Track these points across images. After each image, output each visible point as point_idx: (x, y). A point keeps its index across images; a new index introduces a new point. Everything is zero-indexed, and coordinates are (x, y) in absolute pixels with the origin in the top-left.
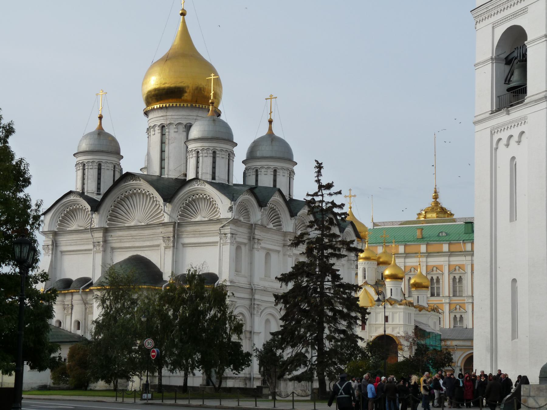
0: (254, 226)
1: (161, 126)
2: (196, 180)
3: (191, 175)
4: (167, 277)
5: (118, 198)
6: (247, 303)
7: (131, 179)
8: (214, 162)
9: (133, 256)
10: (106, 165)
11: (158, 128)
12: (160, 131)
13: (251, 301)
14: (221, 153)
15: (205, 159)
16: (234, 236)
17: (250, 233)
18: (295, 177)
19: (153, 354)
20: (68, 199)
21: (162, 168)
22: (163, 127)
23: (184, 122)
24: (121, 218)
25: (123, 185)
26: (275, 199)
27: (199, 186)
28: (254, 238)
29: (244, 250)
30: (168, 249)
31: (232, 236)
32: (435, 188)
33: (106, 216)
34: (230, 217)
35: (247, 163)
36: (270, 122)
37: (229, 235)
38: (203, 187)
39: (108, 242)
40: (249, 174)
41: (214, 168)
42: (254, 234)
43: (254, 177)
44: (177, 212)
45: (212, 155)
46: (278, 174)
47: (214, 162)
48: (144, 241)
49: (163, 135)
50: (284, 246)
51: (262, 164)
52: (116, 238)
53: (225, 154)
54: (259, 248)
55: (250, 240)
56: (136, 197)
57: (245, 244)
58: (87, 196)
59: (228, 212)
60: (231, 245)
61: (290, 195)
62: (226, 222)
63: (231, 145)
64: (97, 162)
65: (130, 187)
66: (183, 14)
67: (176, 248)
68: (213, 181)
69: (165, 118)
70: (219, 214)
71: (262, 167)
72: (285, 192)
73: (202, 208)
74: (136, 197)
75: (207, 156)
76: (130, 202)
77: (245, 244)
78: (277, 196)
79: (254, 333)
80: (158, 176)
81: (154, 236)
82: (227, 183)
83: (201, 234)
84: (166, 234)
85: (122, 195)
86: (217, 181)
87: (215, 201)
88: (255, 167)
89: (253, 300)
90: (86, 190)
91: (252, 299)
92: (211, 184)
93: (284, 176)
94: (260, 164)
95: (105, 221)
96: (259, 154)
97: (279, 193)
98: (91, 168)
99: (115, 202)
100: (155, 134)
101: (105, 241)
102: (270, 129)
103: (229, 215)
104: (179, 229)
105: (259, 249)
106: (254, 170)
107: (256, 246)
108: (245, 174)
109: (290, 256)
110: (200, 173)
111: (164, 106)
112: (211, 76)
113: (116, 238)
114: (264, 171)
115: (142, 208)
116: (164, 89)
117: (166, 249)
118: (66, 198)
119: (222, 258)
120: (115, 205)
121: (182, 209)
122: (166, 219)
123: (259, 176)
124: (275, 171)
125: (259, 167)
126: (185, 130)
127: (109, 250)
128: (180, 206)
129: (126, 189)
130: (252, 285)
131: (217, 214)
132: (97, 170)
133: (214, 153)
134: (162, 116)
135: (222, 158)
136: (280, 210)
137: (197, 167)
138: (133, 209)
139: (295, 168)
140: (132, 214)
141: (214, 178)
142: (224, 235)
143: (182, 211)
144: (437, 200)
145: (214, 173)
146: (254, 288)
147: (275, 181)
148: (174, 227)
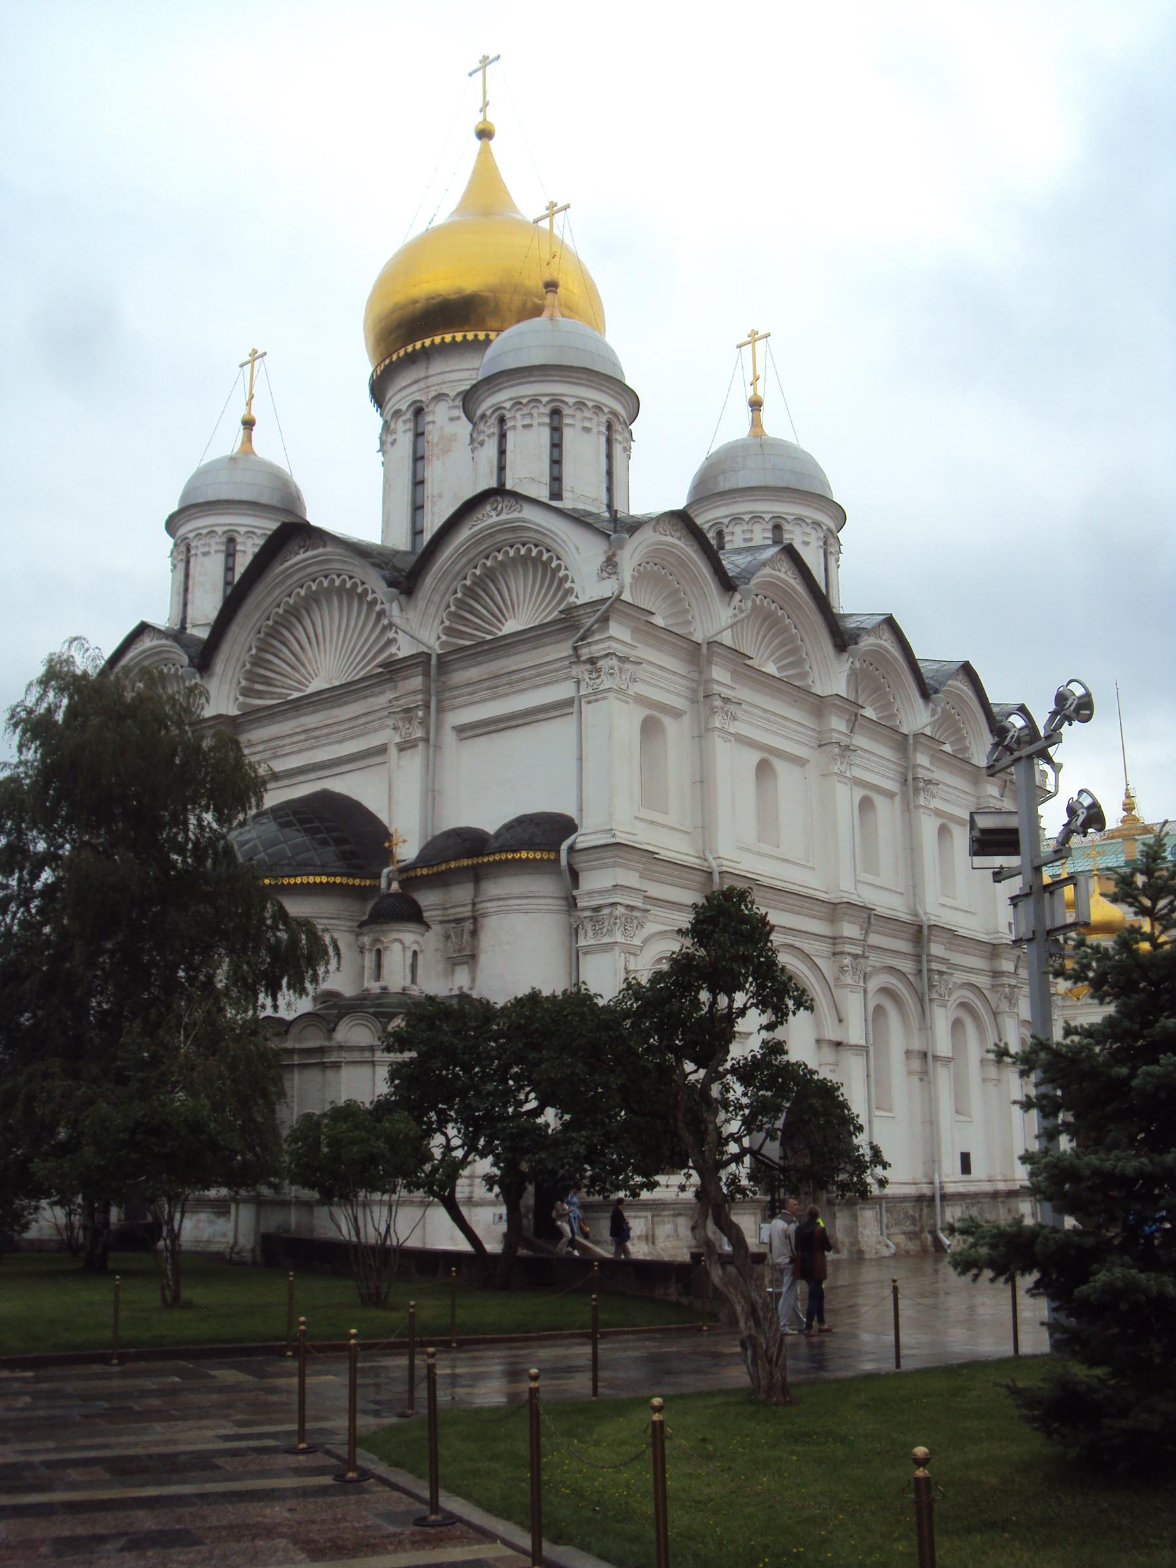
1: (412, 409)
2: (492, 499)
4: (408, 850)
5: (268, 619)
7: (301, 547)
8: (556, 445)
10: (250, 542)
14: (579, 414)
15: (529, 435)
16: (627, 666)
20: (137, 651)
25: (277, 571)
26: (779, 578)
27: (504, 517)
30: (409, 752)
32: (1127, 790)
33: (235, 681)
38: (515, 515)
41: (556, 462)
44: (437, 621)
45: (547, 420)
47: (556, 445)
48: (342, 741)
49: (419, 435)
50: (820, 746)
51: (735, 512)
52: (260, 748)
53: (595, 417)
55: (694, 701)
56: (320, 609)
57: (676, 714)
62: (593, 619)
65: (295, 578)
66: (485, 134)
68: (554, 504)
69: (422, 385)
71: (736, 519)
74: (320, 609)
75: (530, 426)
76: (305, 630)
77: (676, 714)
78: (786, 573)
81: (370, 718)
83: (515, 682)
84: (401, 702)
85: (278, 606)
86: (567, 503)
87: (558, 558)
95: (232, 697)
98: (206, 554)
99: (259, 632)
100: (395, 440)
102: (756, 423)
104: (443, 679)
113: (260, 748)
114: (743, 531)
117: (403, 753)
118: (132, 649)
120: (258, 644)
121: (453, 608)
125: (726, 521)
129: (289, 582)
130: (710, 858)
132: (221, 557)
133: (556, 413)
134: (416, 382)
135: (587, 430)
136: (800, 627)
138: (312, 650)
140: (310, 664)
141: (556, 495)
142: (588, 667)
143: (454, 616)
144: (1133, 813)
145: (556, 480)
146: (716, 869)
148: (426, 674)
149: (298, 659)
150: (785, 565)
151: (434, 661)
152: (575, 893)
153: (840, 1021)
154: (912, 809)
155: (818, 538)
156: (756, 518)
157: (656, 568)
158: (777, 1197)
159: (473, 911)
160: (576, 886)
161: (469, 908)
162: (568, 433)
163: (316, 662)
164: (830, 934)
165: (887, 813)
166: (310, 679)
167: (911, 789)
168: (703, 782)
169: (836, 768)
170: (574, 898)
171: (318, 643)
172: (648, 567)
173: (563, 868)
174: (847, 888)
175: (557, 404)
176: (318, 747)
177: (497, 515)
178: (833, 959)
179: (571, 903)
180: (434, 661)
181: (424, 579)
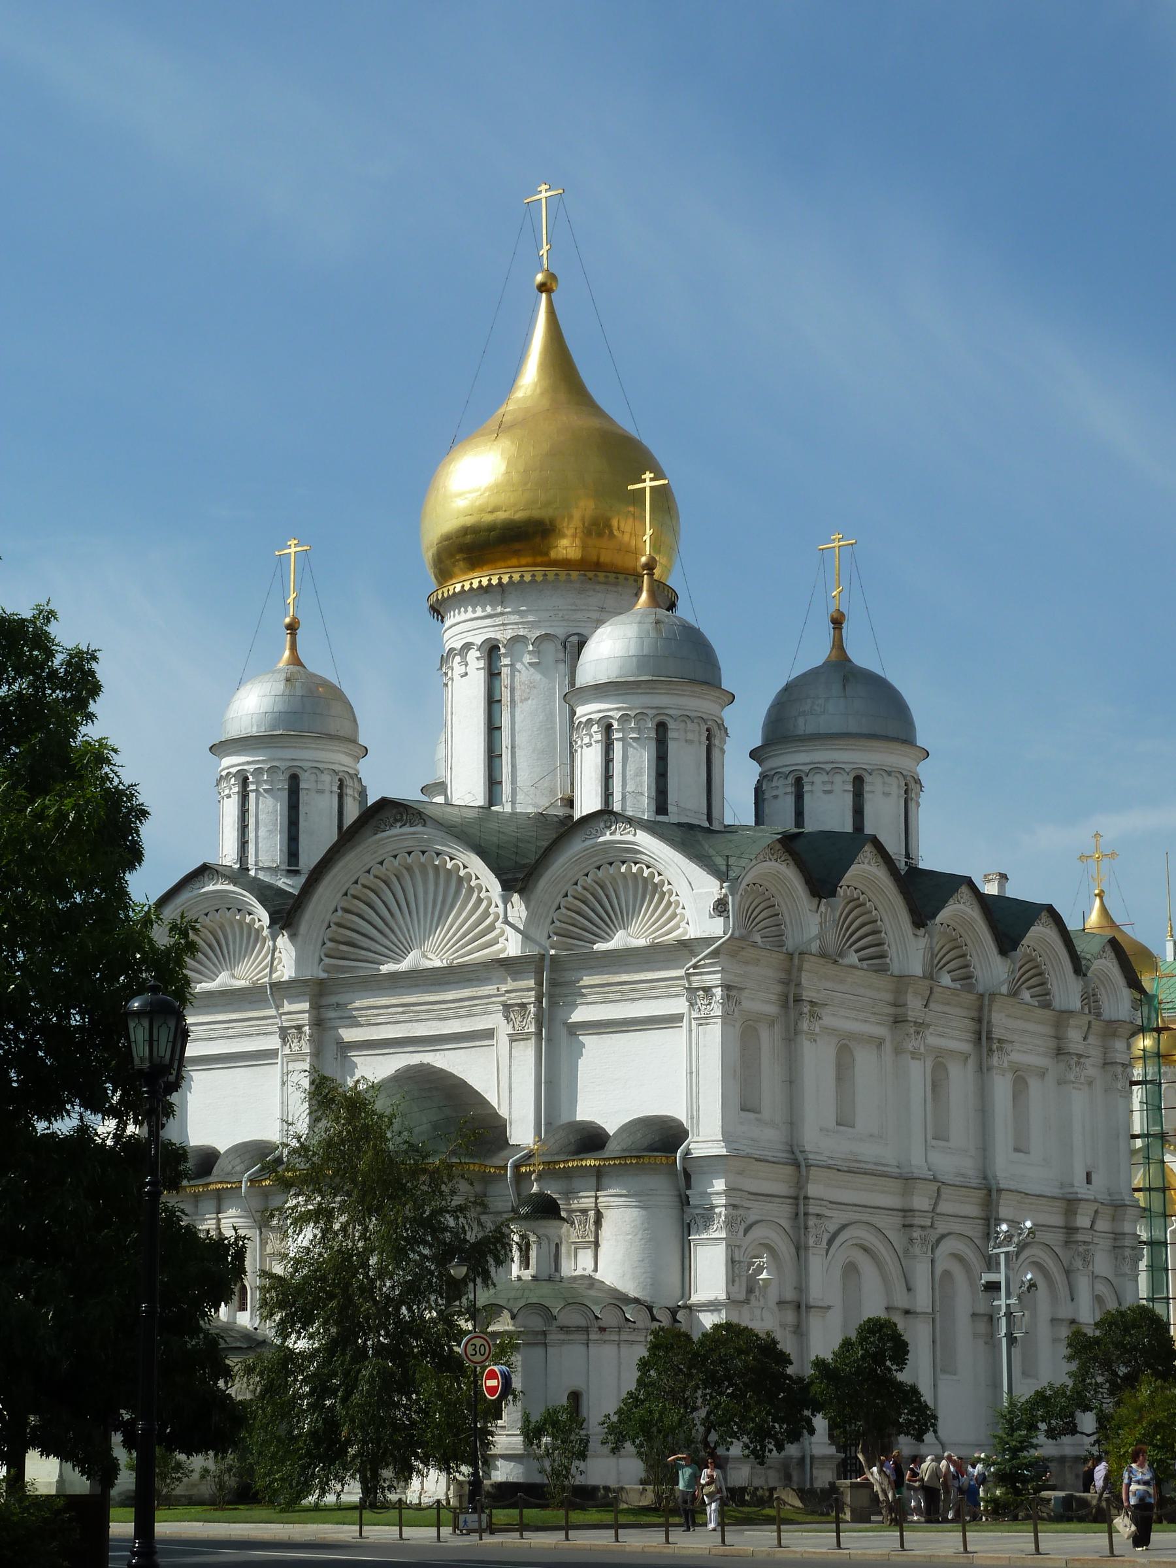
0: (796, 957)
1: (487, 647)
2: (606, 817)
3: (588, 802)
6: (781, 1213)
7: (396, 821)
8: (661, 759)
9: (409, 1068)
11: (478, 654)
12: (482, 664)
13: (797, 1205)
17: (786, 983)
18: (924, 799)
19: (492, 1383)
21: (493, 783)
22: (491, 651)
23: (560, 631)
24: (365, 946)
27: (617, 837)
28: (798, 1000)
29: (769, 1041)
30: (522, 1042)
31: (728, 996)
34: (719, 932)
35: (767, 758)
36: (837, 622)
37: (718, 992)
39: (328, 1025)
40: (775, 793)
42: (798, 985)
43: (789, 802)
46: (867, 788)
48: (445, 1019)
49: (493, 675)
50: (896, 1022)
54: (817, 1030)
58: (255, 878)
59: (711, 917)
60: (723, 1024)
61: (908, 856)
63: (713, 701)
64: (283, 768)
67: (549, 1040)
68: (661, 818)
69: (499, 621)
70: (683, 924)
71: (817, 770)
72: (894, 847)
73: (627, 906)
78: (869, 863)
79: (808, 1307)
80: (479, 807)
82: (706, 825)
83: (627, 993)
86: (673, 817)
87: (669, 884)
88: (793, 768)
89: (801, 1202)
90: (251, 860)
91: (798, 1201)
92: (651, 828)
93: (886, 794)
94: (808, 761)
96: (804, 726)
97: (875, 852)
100: (466, 674)
101: (319, 1023)
102: (838, 645)
103: (716, 928)
105: (816, 1034)
106: (791, 780)
107: (805, 1025)
108: (759, 791)
109: (915, 1055)
110: (617, 796)
111: (495, 581)
112: (644, 481)
115: (433, 913)
116: (491, 527)
117: (513, 1044)
118: (189, 889)
119: (698, 1071)
122: (512, 946)
123: (807, 797)
124: (858, 781)
126: (561, 656)
127: (331, 1051)
128: (555, 906)
131: (677, 927)
136: (880, 908)
137: (608, 777)
138: (404, 918)
139: (924, 770)
147: (858, 812)
149: (387, 924)
150: (868, 853)
151: (547, 962)
152: (688, 1192)
153: (909, 1290)
154: (985, 1070)
155: (899, 786)
156: (838, 770)
157: (755, 888)
158: (848, 1455)
159: (596, 1203)
160: (689, 1187)
161: (593, 1200)
162: (672, 747)
163: (409, 930)
164: (899, 1206)
165: (960, 1078)
166: (410, 950)
167: (985, 1050)
168: (792, 1081)
169: (911, 1045)
170: (688, 1197)
171: (419, 921)
172: (749, 889)
173: (678, 1173)
174: (917, 1162)
175: (667, 718)
176: (417, 1021)
177: (611, 834)
178: (902, 1231)
179: (684, 1201)
180: (547, 962)
181: (538, 880)
